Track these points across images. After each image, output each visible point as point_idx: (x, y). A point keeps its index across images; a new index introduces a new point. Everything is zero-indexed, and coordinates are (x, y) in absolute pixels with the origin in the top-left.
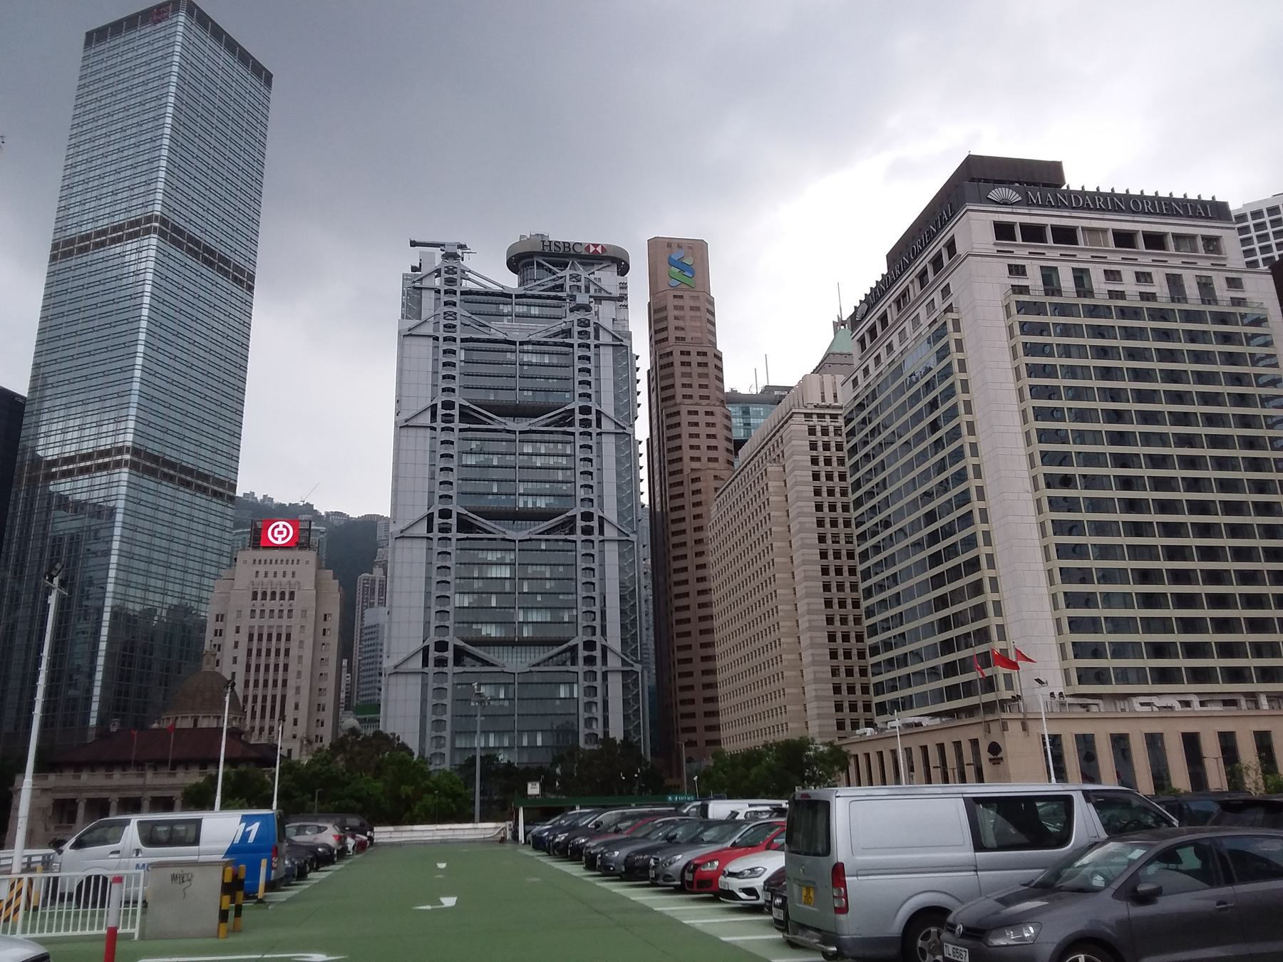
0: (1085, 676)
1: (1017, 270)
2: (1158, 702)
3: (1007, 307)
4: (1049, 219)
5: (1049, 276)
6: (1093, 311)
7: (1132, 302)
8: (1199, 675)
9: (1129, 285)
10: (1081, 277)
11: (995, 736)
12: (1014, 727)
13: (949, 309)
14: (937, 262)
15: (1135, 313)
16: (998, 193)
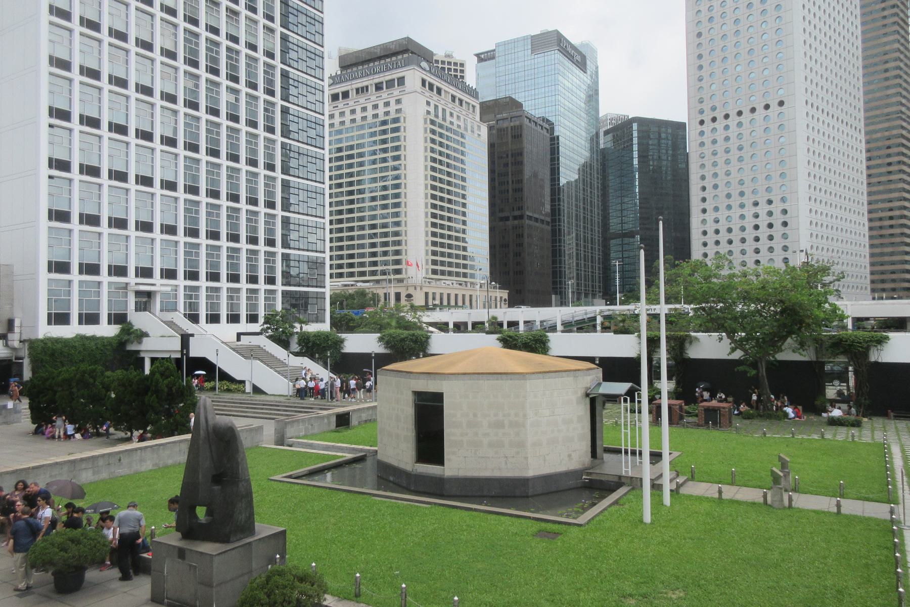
0: (434, 272)
1: (428, 103)
2: (447, 282)
3: (425, 120)
4: (437, 83)
5: (436, 107)
6: (448, 129)
7: (455, 127)
8: (458, 274)
9: (454, 120)
10: (444, 110)
11: (411, 291)
12: (418, 289)
13: (398, 111)
14: (390, 84)
15: (455, 133)
16: (424, 64)
